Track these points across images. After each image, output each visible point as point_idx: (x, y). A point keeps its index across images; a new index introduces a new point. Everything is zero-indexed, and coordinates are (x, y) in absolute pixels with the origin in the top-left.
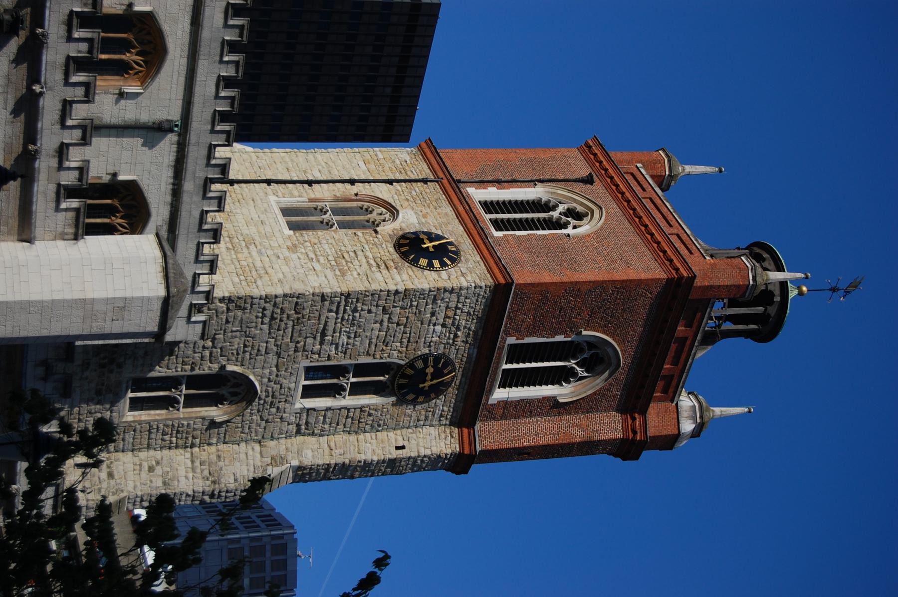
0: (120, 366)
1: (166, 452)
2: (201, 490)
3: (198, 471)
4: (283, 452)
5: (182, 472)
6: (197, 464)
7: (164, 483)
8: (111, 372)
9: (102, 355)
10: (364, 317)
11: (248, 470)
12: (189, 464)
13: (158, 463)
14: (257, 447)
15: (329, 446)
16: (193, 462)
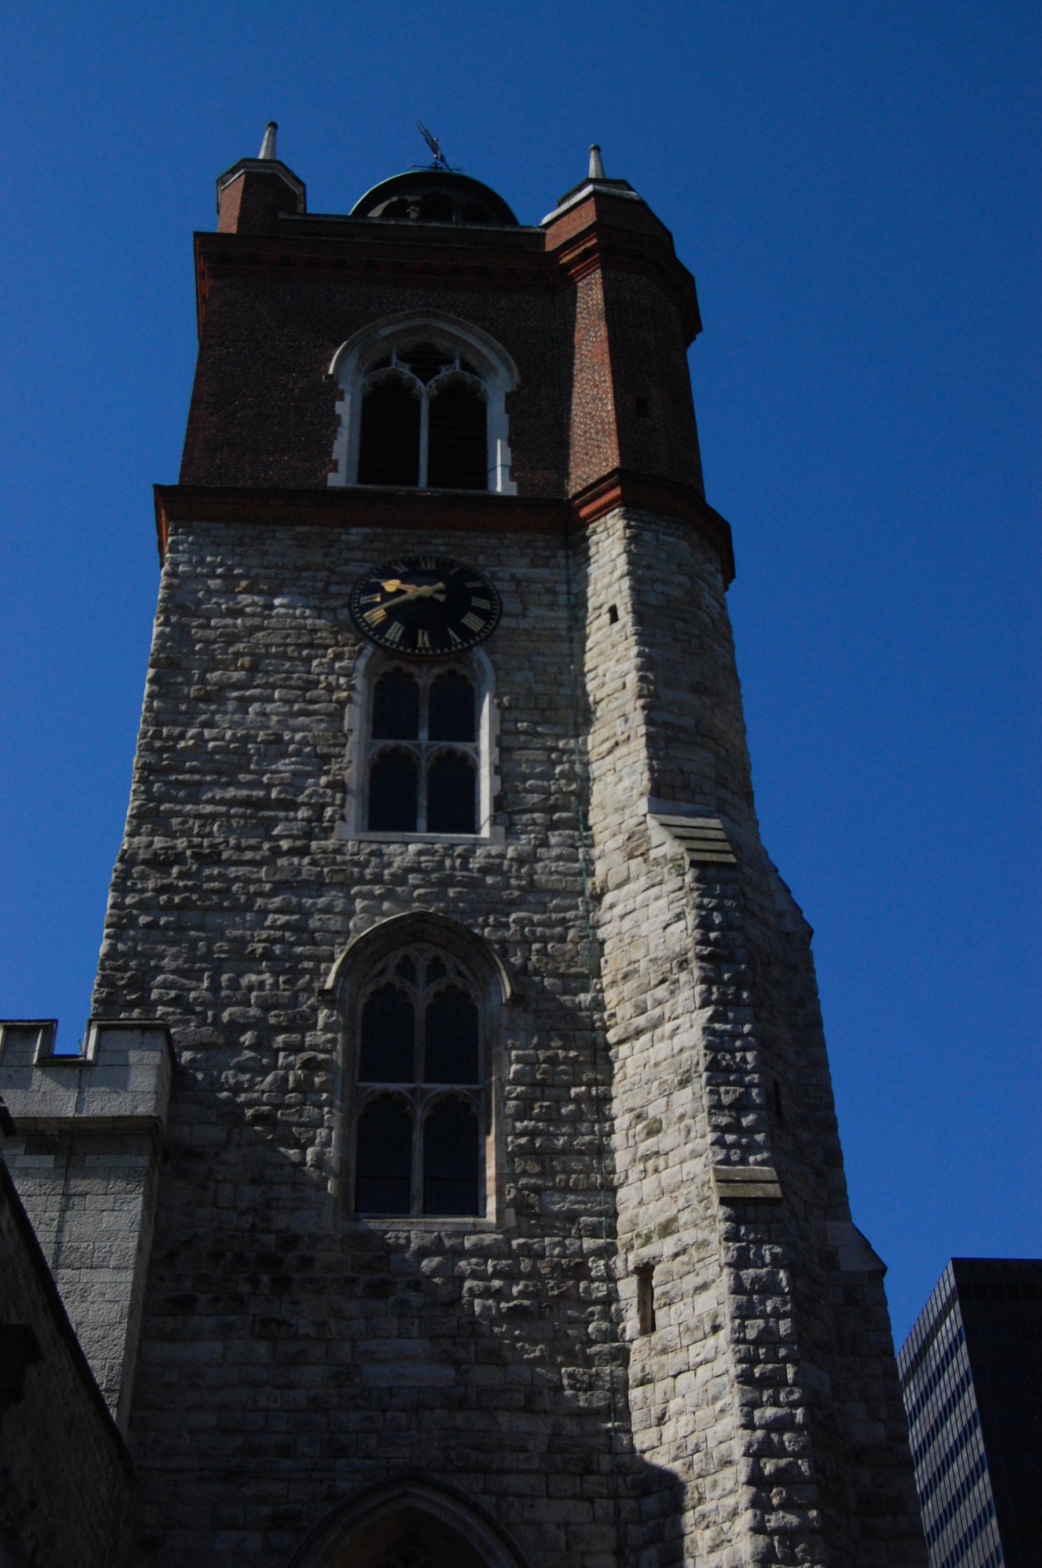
0: (290, 1240)
1: (616, 1107)
2: (700, 988)
3: (657, 1011)
4: (621, 839)
5: (662, 1049)
6: (641, 1021)
7: (683, 1083)
8: (306, 1262)
9: (244, 1289)
10: (222, 730)
11: (657, 898)
12: (645, 1038)
13: (639, 1117)
14: (607, 900)
15: (610, 752)
16: (639, 1033)
